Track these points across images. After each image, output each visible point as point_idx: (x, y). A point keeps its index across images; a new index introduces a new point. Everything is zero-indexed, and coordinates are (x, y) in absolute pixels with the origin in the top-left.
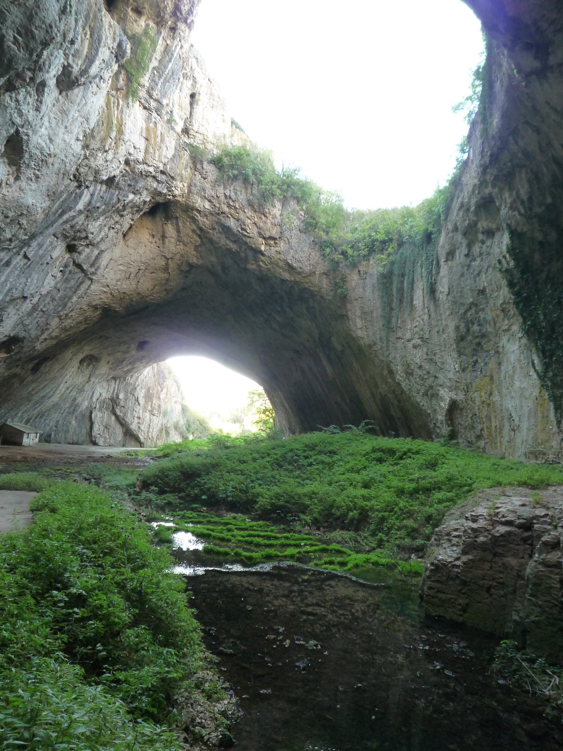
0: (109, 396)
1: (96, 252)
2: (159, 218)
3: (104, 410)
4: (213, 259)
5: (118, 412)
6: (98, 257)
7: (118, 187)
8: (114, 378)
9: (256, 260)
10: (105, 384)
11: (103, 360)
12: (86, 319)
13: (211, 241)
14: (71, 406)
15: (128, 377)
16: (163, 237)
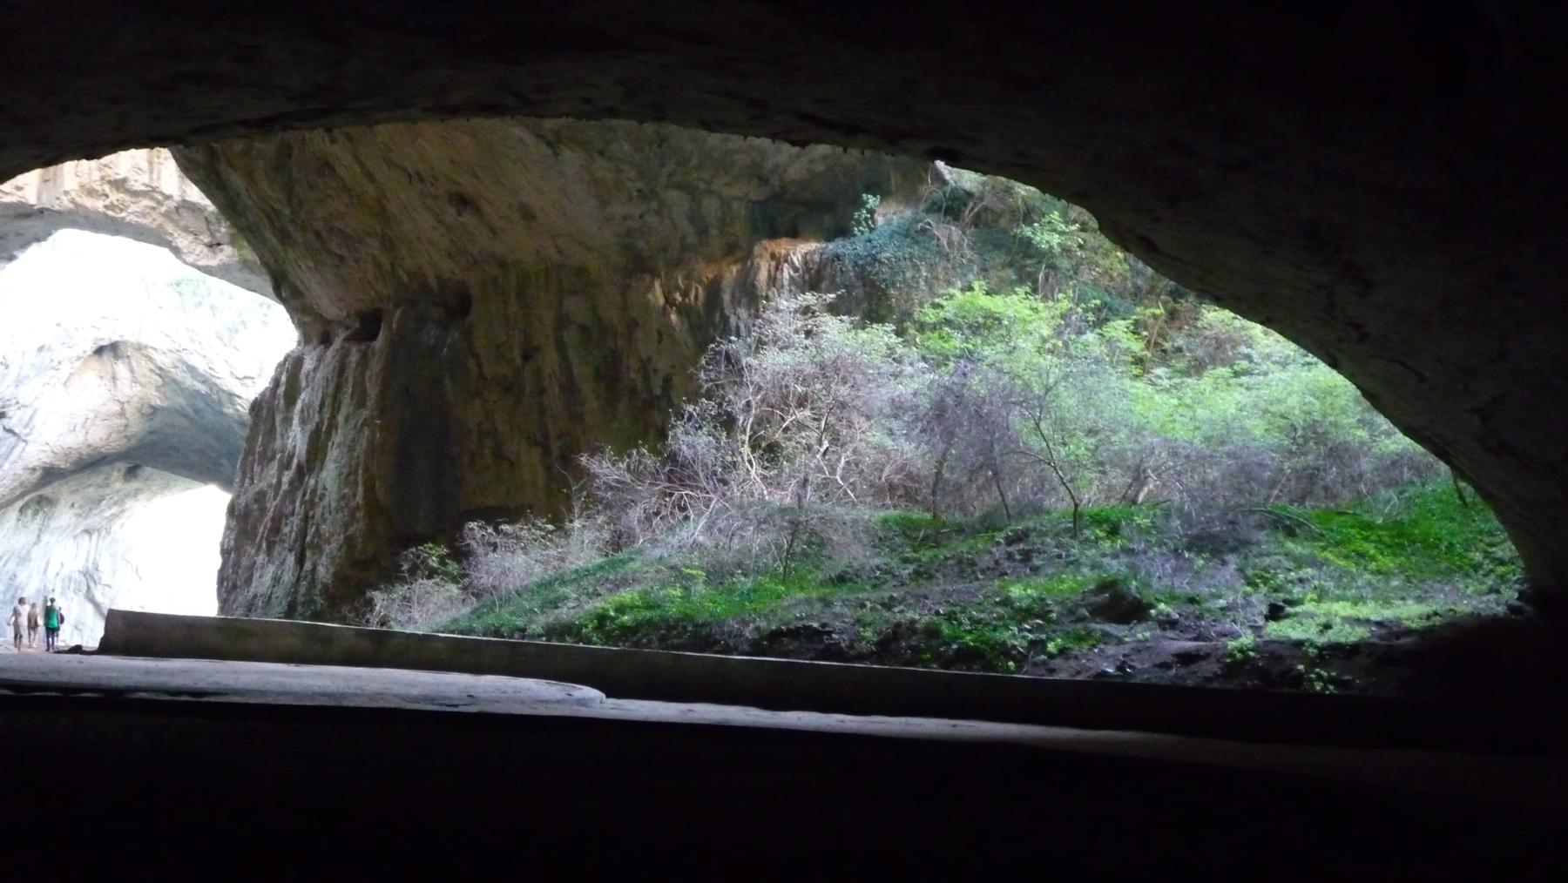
0: (79, 565)
1: (29, 412)
2: (107, 356)
3: (70, 594)
4: (182, 401)
5: (99, 598)
6: (31, 418)
7: (49, 349)
8: (88, 532)
9: (233, 403)
10: (69, 542)
11: (63, 502)
12: (22, 484)
13: (174, 381)
14: (8, 589)
15: (115, 527)
16: (114, 378)
